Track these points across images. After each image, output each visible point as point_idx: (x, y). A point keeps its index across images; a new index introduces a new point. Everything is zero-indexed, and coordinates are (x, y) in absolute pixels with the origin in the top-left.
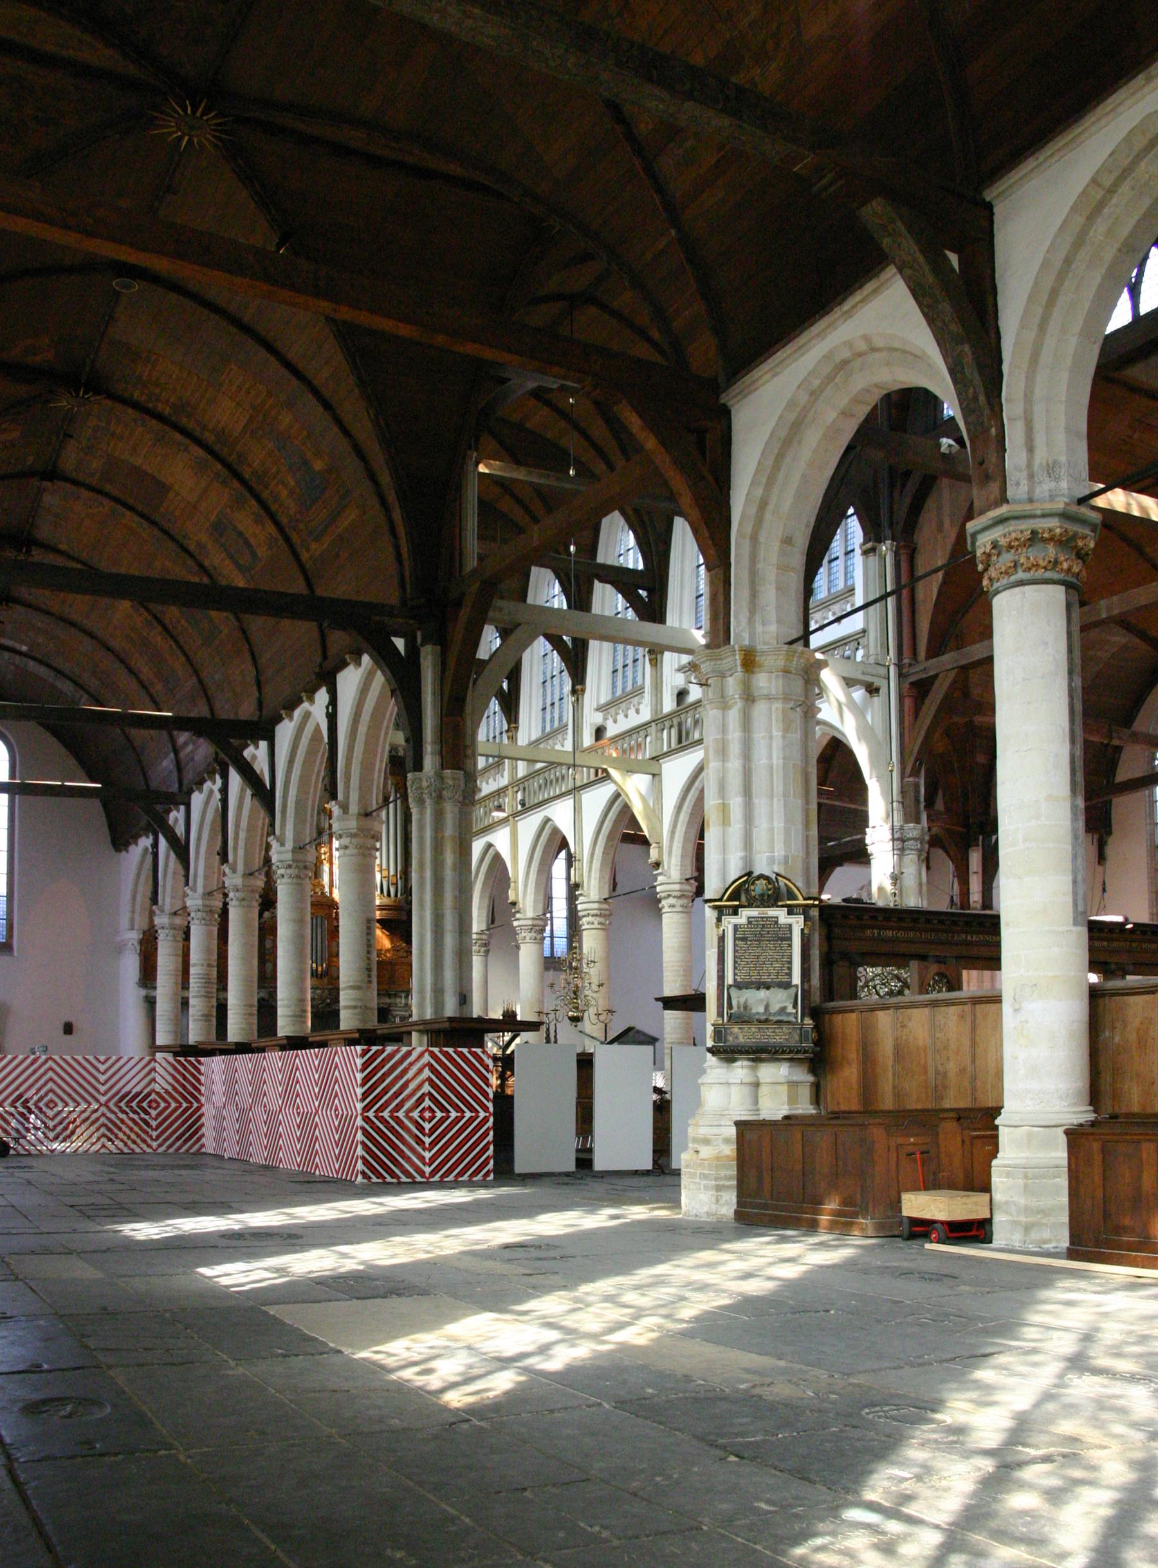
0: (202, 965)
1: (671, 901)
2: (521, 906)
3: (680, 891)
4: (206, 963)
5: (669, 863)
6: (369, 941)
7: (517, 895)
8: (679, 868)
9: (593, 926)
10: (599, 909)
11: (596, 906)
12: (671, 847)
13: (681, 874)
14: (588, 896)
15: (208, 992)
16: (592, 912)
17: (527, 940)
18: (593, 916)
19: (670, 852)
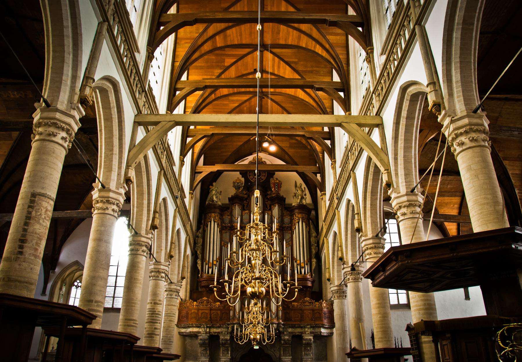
0: (151, 303)
1: (404, 210)
2: (345, 260)
3: (408, 201)
4: (153, 302)
5: (397, 183)
6: (30, 213)
7: (342, 253)
8: (404, 184)
9: (371, 256)
10: (373, 243)
11: (371, 241)
12: (396, 170)
13: (407, 188)
14: (366, 236)
15: (151, 319)
16: (369, 246)
17: (351, 280)
18: (370, 248)
19: (397, 174)
